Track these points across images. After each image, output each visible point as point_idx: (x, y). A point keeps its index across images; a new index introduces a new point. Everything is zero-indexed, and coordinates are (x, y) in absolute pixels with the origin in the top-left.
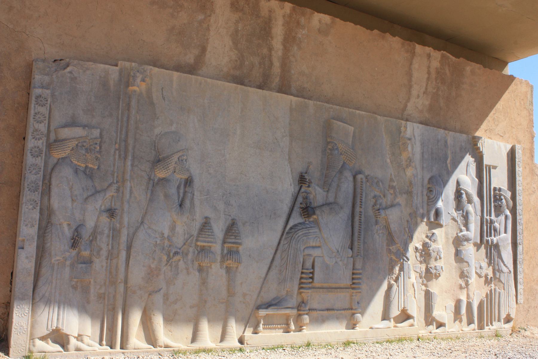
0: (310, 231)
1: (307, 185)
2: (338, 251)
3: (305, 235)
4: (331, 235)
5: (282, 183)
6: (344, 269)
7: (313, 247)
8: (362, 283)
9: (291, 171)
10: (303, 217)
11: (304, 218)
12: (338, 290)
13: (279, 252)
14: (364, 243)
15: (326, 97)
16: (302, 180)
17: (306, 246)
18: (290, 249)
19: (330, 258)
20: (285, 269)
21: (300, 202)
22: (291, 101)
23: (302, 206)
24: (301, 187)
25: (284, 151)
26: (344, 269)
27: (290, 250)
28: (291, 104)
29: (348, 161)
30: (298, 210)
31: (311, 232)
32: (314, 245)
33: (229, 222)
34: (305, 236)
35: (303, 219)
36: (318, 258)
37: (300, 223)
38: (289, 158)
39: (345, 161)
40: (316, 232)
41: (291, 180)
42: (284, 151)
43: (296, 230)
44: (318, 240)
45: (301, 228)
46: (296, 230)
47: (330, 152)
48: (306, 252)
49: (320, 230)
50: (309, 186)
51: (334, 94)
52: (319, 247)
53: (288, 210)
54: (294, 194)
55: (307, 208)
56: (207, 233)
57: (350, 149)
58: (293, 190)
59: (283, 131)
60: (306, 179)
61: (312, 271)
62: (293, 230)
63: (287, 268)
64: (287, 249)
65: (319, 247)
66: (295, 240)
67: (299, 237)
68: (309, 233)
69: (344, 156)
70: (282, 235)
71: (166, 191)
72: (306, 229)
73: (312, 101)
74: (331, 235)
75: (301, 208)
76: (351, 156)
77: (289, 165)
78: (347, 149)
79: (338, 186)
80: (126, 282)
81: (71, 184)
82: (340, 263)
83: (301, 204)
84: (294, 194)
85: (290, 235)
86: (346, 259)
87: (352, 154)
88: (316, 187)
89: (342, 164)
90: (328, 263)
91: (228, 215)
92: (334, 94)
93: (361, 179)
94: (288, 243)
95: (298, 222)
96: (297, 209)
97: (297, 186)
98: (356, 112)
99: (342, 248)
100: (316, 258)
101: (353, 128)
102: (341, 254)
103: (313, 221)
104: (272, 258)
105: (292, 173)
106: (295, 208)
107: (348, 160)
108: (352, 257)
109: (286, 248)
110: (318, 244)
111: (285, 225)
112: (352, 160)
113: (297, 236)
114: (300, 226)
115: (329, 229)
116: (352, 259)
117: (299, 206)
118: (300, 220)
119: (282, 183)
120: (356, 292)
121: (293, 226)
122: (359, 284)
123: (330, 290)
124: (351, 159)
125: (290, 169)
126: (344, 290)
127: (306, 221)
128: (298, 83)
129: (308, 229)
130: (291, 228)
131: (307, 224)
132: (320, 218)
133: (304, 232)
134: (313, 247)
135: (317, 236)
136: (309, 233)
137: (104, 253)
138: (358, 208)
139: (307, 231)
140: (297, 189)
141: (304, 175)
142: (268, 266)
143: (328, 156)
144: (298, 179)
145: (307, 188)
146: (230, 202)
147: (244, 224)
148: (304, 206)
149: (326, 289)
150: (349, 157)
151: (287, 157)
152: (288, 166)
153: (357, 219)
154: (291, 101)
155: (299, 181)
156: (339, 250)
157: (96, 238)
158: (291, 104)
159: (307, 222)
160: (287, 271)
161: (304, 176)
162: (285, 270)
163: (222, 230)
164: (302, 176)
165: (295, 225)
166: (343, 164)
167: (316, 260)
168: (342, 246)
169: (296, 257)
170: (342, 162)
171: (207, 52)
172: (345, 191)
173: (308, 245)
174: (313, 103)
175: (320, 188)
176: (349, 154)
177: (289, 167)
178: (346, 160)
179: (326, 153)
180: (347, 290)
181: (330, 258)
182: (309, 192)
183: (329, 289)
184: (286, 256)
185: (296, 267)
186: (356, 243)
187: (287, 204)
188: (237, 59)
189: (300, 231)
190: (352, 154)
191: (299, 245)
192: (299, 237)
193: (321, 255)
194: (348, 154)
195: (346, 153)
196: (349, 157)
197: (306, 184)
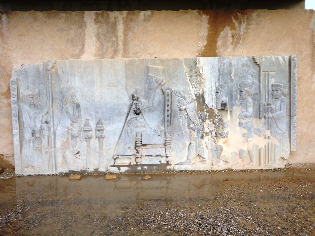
0: (139, 121)
16: (133, 98)
22: (125, 61)
28: (125, 62)
33: (98, 120)
37: (134, 118)
38: (126, 88)
49: (144, 120)
53: (127, 112)
56: (87, 126)
58: (129, 103)
79: (154, 98)
81: (28, 112)
96: (132, 111)
104: (120, 134)
106: (131, 111)
125: (127, 93)
130: (129, 120)
137: (46, 137)
142: (118, 138)
147: (105, 120)
151: (125, 88)
154: (125, 61)
157: (42, 131)
163: (95, 124)
171: (85, 46)
177: (126, 92)
188: (100, 46)
197: (135, 99)
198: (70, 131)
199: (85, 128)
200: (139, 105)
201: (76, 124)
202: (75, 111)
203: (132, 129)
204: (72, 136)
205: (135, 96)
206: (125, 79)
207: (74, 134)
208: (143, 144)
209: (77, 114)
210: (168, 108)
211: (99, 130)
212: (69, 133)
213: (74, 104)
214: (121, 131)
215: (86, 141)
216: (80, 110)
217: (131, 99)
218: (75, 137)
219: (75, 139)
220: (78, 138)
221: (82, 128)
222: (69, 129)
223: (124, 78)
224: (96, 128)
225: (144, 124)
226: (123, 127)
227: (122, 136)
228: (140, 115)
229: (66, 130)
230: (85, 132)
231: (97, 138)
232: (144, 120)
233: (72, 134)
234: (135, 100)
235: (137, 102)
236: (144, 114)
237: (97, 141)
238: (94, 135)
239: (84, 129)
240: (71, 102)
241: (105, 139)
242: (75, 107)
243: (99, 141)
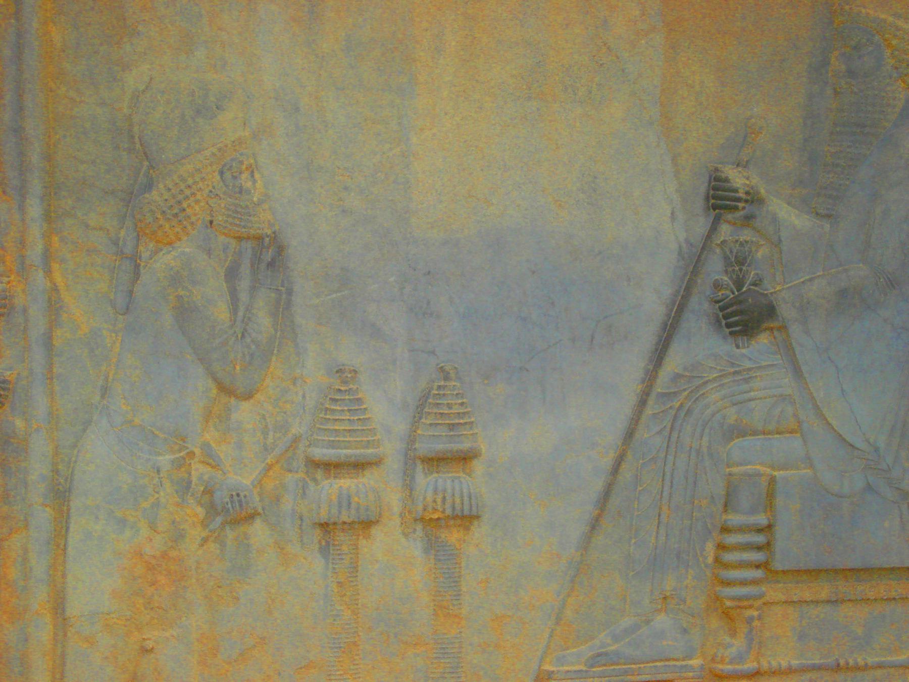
4: (842, 390)
10: (727, 331)
11: (731, 333)
27: (670, 458)
30: (706, 305)
58: (682, 236)
64: (662, 455)
70: (642, 403)
71: (182, 292)
74: (842, 390)
80: (59, 606)
91: (423, 351)
94: (666, 434)
144: (703, 189)
146: (428, 303)
155: (707, 198)
164: (717, 179)
169: (695, 483)
189: (710, 386)
198: (198, 470)
199: (332, 445)
200: (759, 255)
201: (246, 405)
202: (244, 297)
203: (705, 450)
204: (212, 509)
205: (738, 179)
207: (237, 497)
208: (778, 565)
209: (263, 321)
211: (436, 461)
212: (185, 487)
213: (239, 239)
214: (607, 461)
215: (324, 550)
216: (290, 292)
217: (699, 203)
218: (236, 522)
219: (230, 534)
220: (258, 524)
221: (296, 440)
222: (191, 454)
224: (411, 439)
225: (790, 410)
226: (629, 435)
228: (763, 340)
229: (165, 460)
230: (319, 474)
231: (419, 527)
233: (209, 491)
234: (730, 217)
235: (746, 235)
236: (795, 330)
237: (414, 549)
238: (394, 499)
239: (318, 453)
240: (219, 219)
241: (480, 532)
242: (245, 269)
243: (432, 546)
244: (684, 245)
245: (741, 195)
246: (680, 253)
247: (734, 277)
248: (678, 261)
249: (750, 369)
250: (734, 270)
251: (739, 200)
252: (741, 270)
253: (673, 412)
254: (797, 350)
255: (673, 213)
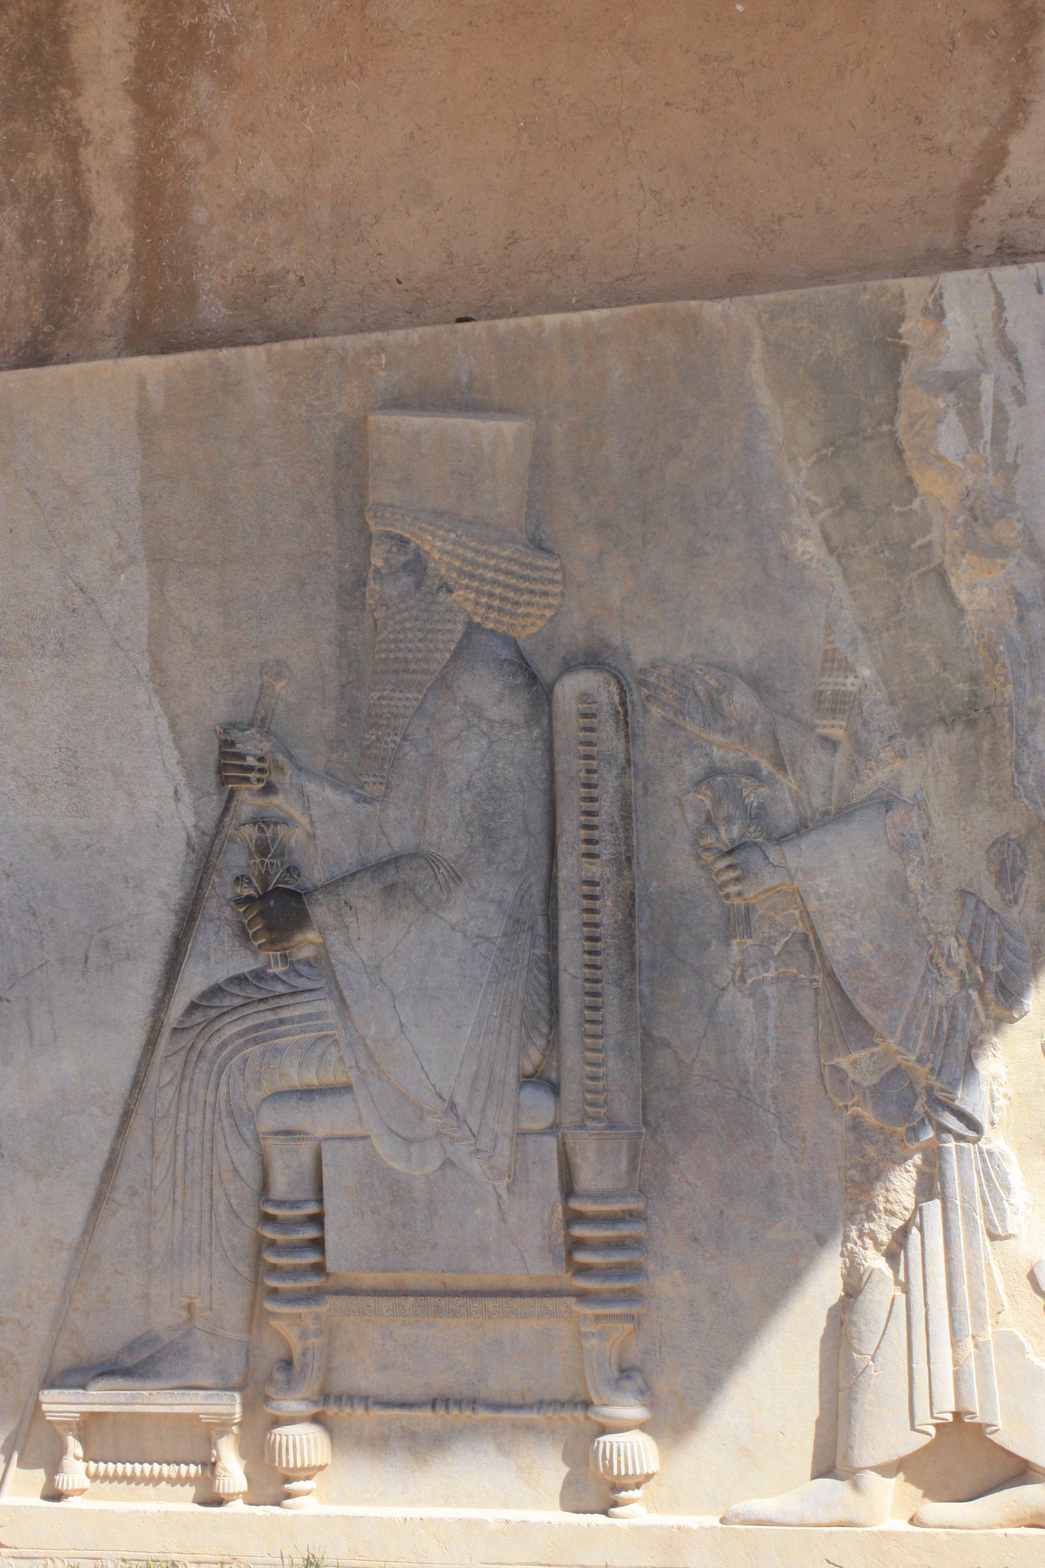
0: (285, 1014)
1: (261, 785)
2: (453, 1106)
3: (254, 1036)
4: (402, 1025)
5: (131, 795)
6: (505, 1196)
7: (308, 1093)
8: (651, 1266)
9: (173, 726)
12: (490, 1303)
13: (139, 1123)
14: (650, 1044)
15: (406, 285)
17: (267, 1088)
18: (184, 1107)
19: (408, 1141)
20: (171, 1204)
21: (237, 872)
22: (142, 383)
23: (247, 892)
24: (232, 794)
25: (128, 639)
26: (505, 1196)
27: (183, 1115)
28: (143, 399)
29: (493, 615)
30: (228, 912)
31: (291, 1020)
32: (311, 1078)
34: (255, 1041)
35: (254, 953)
36: (337, 1143)
37: (239, 980)
38: (157, 666)
39: (477, 619)
40: (318, 1016)
41: (177, 770)
42: (128, 639)
43: (214, 1013)
44: (333, 1050)
45: (237, 1002)
46: (214, 1013)
47: (378, 588)
48: (270, 1119)
50: (269, 789)
51: (450, 255)
52: (347, 1088)
53: (173, 919)
54: (195, 840)
55: (265, 896)
57: (495, 550)
58: (190, 820)
59: (112, 540)
60: (242, 756)
61: (311, 1209)
62: (198, 1017)
63: (174, 1202)
64: (173, 1110)
65: (347, 1088)
66: (204, 1065)
67: (224, 1045)
68: (282, 1022)
69: (461, 593)
72: (263, 1006)
73: (260, 348)
74: (402, 1025)
75: (240, 901)
76: (507, 586)
77: (156, 701)
78: (470, 555)
82: (475, 1166)
83: (238, 880)
84: (195, 840)
85: (183, 1043)
86: (504, 1146)
87: (508, 573)
88: (312, 787)
89: (459, 636)
90: (399, 1166)
92: (450, 255)
93: (584, 697)
94: (176, 1082)
95: (232, 973)
97: (215, 797)
98: (540, 324)
99: (473, 1087)
100: (325, 1147)
101: (509, 427)
102: (474, 1122)
103: (316, 959)
105: (177, 739)
107: (489, 607)
108: (554, 1128)
109: (167, 1105)
110: (333, 1076)
111: (160, 995)
112: (517, 603)
113: (216, 1043)
114: (236, 990)
115: (394, 997)
116: (551, 1144)
117: (229, 895)
118: (243, 963)
119: (131, 795)
120: (597, 1318)
121: (204, 996)
122: (634, 1270)
123: (443, 1302)
124: (503, 599)
125: (164, 722)
126: (529, 1301)
127: (270, 967)
128: (230, 265)
129: (273, 1003)
131: (276, 977)
132: (335, 941)
133: (249, 1023)
134: (308, 1093)
135: (326, 1036)
136: (282, 1022)
138: (571, 860)
139: (270, 1017)
140: (213, 806)
141: (235, 735)
143: (373, 611)
145: (260, 801)
148: (252, 892)
149: (411, 1299)
150: (491, 595)
151: (145, 667)
152: (150, 707)
153: (569, 919)
154: (142, 383)
156: (461, 1100)
158: (143, 399)
159: (278, 969)
160: (179, 1212)
161: (233, 743)
162: (170, 1209)
165: (216, 991)
166: (467, 634)
167: (327, 1157)
168: (476, 1078)
170: (460, 628)
172: (469, 785)
173: (281, 1085)
174: (263, 357)
175: (338, 785)
176: (490, 575)
177: (158, 708)
178: (482, 611)
179: (364, 594)
180: (549, 1303)
181: (408, 1141)
182: (282, 814)
183: (432, 1300)
184: (171, 1142)
185: (217, 1192)
186: (572, 1055)
187: (162, 894)
189: (228, 1019)
190: (508, 573)
191: (223, 1089)
192: (224, 1045)
193: (358, 1131)
194: (483, 580)
195: (471, 576)
196: (491, 595)
197: (247, 780)
206: (141, 573)
210: (595, 870)
223: (133, 560)
226: (138, 1083)
227: (125, 1177)
232: (342, 999)
244: (194, 834)
245: (251, 761)
246: (189, 844)
247: (256, 873)
248: (188, 854)
249: (280, 996)
250: (255, 863)
251: (251, 769)
252: (262, 862)
253: (183, 1053)
254: (339, 969)
255: (176, 792)
